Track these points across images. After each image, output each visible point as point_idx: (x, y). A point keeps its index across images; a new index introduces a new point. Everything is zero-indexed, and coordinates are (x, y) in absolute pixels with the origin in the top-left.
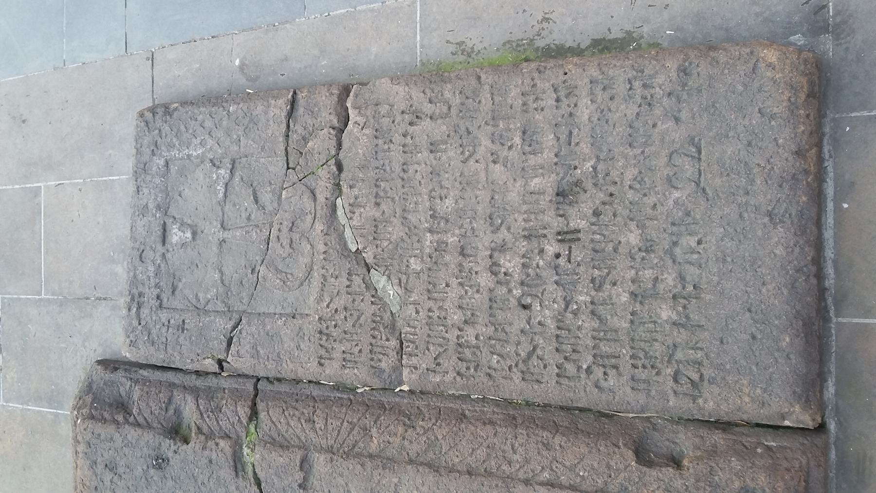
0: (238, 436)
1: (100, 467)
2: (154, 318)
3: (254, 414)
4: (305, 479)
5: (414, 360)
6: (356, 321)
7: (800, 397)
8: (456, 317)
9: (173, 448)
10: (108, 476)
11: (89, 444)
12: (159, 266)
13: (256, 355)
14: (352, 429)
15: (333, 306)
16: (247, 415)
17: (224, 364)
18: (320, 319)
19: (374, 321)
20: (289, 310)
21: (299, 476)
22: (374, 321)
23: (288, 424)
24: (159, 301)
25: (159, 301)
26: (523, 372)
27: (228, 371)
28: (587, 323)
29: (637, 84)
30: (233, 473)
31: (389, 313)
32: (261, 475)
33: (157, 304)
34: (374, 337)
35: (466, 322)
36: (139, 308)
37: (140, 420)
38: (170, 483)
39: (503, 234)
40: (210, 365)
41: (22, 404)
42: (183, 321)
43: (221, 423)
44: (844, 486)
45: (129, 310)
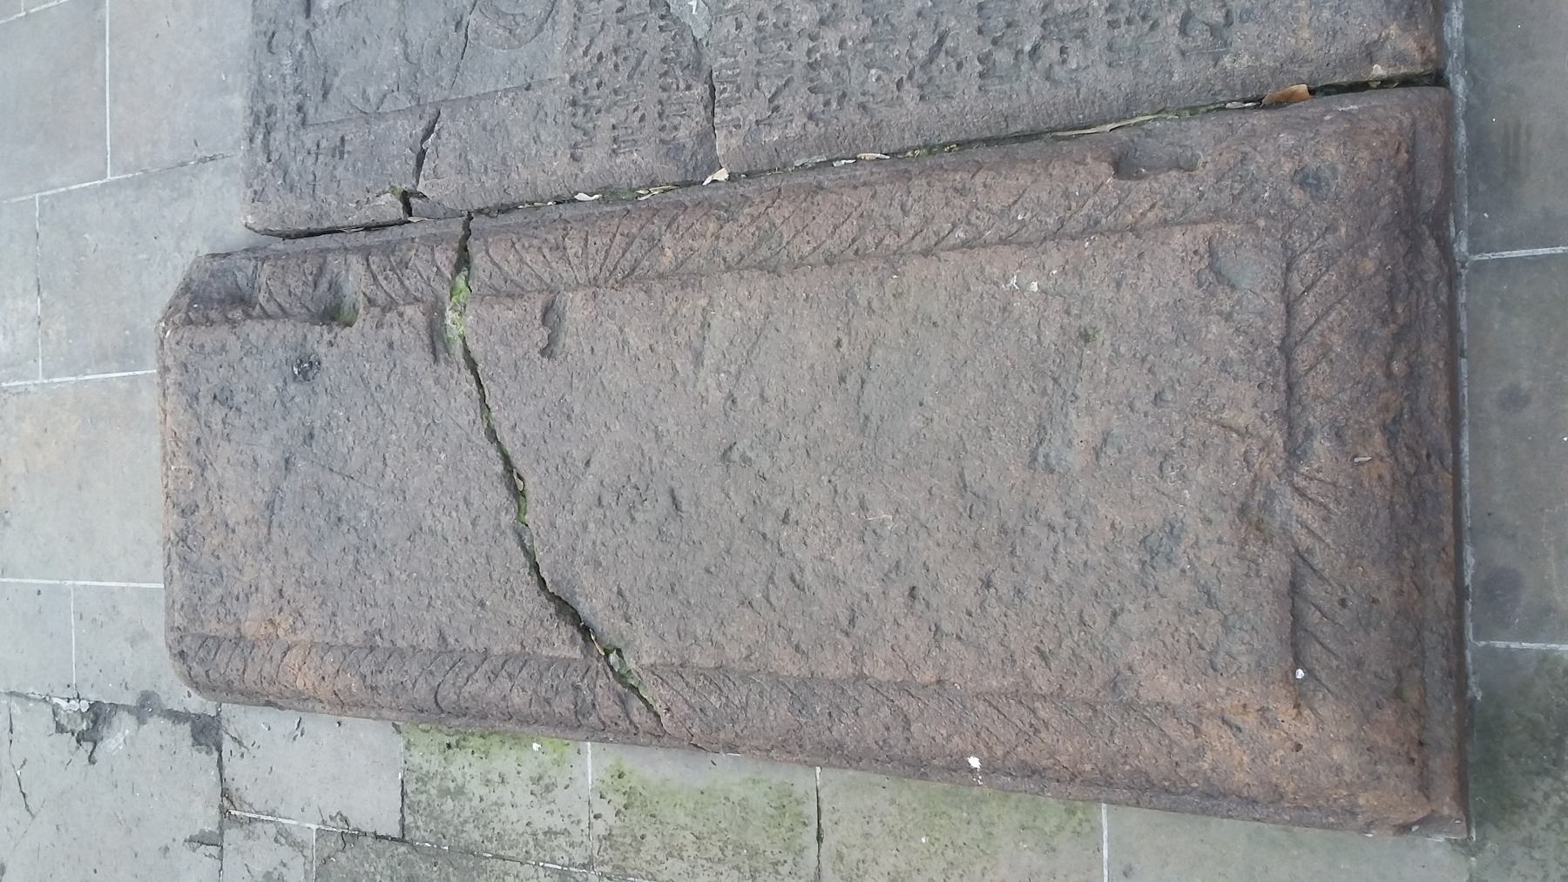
0: (437, 298)
1: (205, 401)
2: (293, 145)
3: (463, 261)
4: (552, 341)
5: (735, 112)
6: (634, 69)
7: (1397, 9)
9: (327, 337)
10: (218, 413)
11: (186, 366)
12: (301, 55)
13: (465, 168)
14: (630, 244)
15: (594, 51)
16: (451, 261)
17: (413, 201)
18: (573, 79)
19: (664, 61)
20: (520, 80)
21: (540, 336)
22: (664, 61)
23: (521, 260)
24: (301, 115)
25: (301, 115)
26: (921, 87)
27: (419, 215)
30: (430, 358)
31: (691, 42)
32: (476, 349)
33: (298, 119)
34: (664, 90)
35: (822, 22)
36: (268, 133)
37: (271, 308)
38: (324, 400)
40: (389, 206)
41: (75, 375)
42: (343, 139)
43: (407, 283)
44: (1482, 187)
45: (251, 141)
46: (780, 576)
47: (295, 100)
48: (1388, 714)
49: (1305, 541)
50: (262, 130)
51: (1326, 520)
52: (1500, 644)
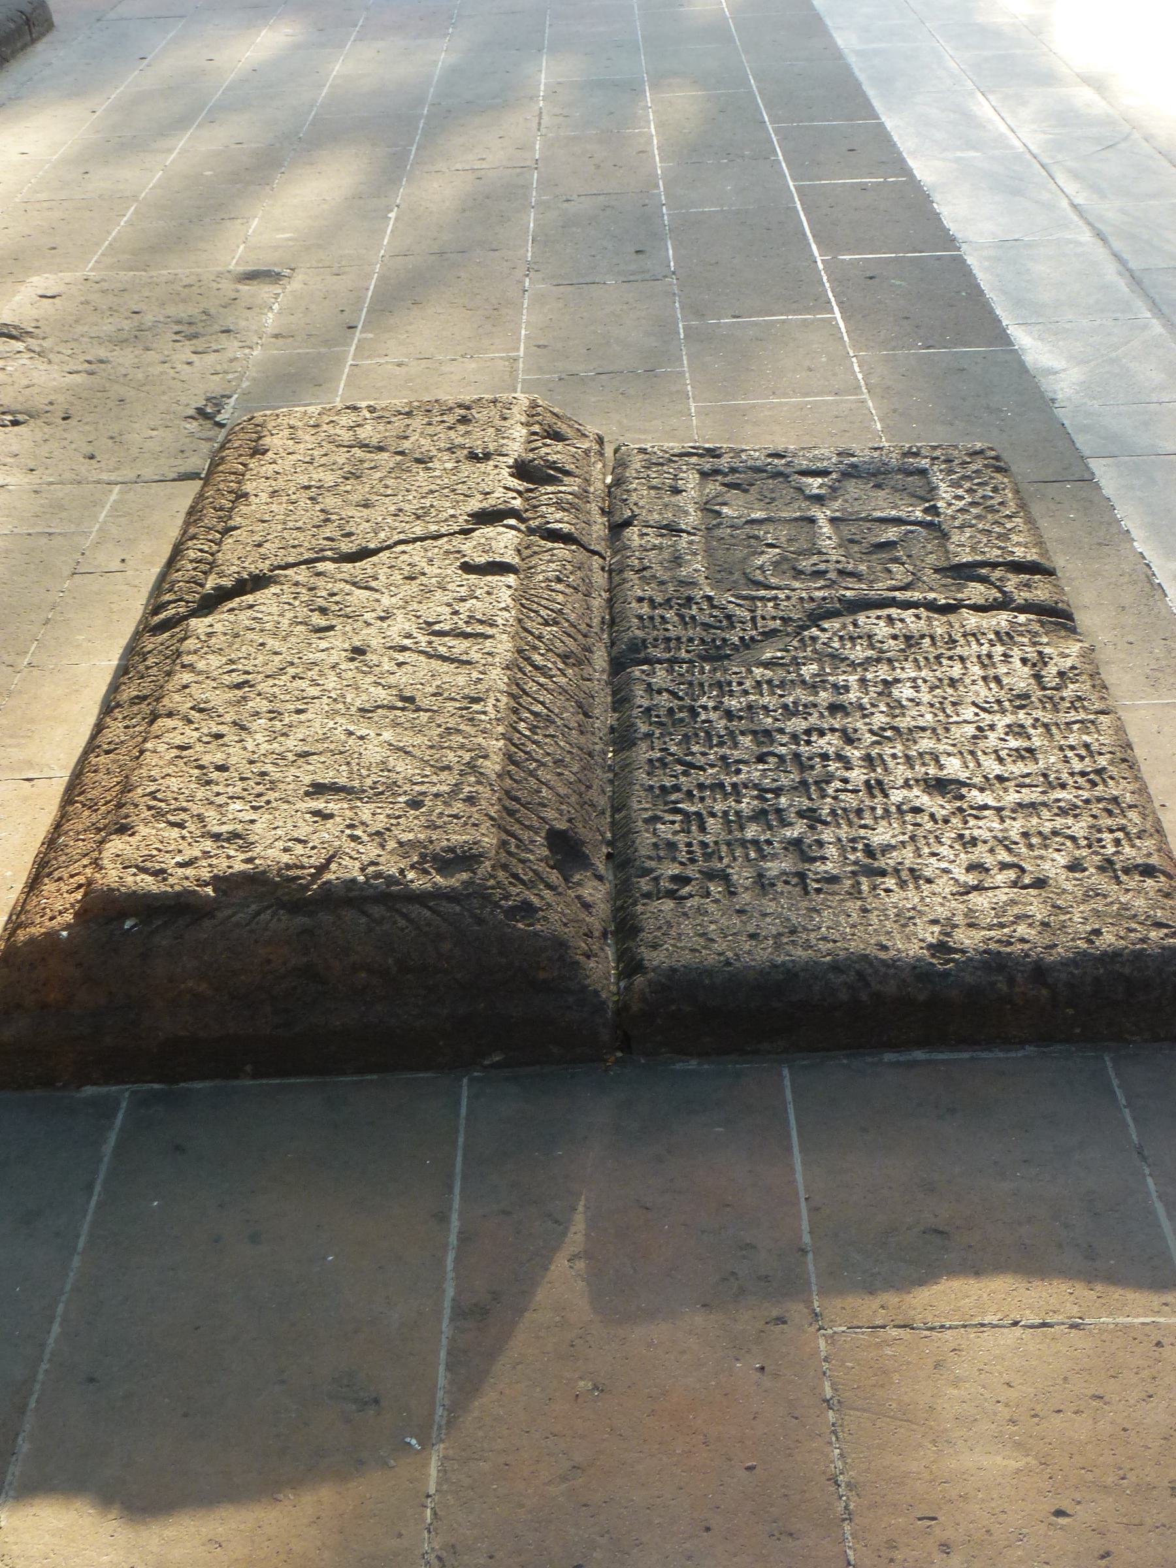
1: (463, 412)
8: (733, 703)
10: (450, 419)
19: (714, 640)
22: (714, 640)
28: (747, 804)
29: (1120, 835)
39: (869, 738)
46: (249, 677)
49: (220, 915)
51: (238, 925)
52: (124, 1105)
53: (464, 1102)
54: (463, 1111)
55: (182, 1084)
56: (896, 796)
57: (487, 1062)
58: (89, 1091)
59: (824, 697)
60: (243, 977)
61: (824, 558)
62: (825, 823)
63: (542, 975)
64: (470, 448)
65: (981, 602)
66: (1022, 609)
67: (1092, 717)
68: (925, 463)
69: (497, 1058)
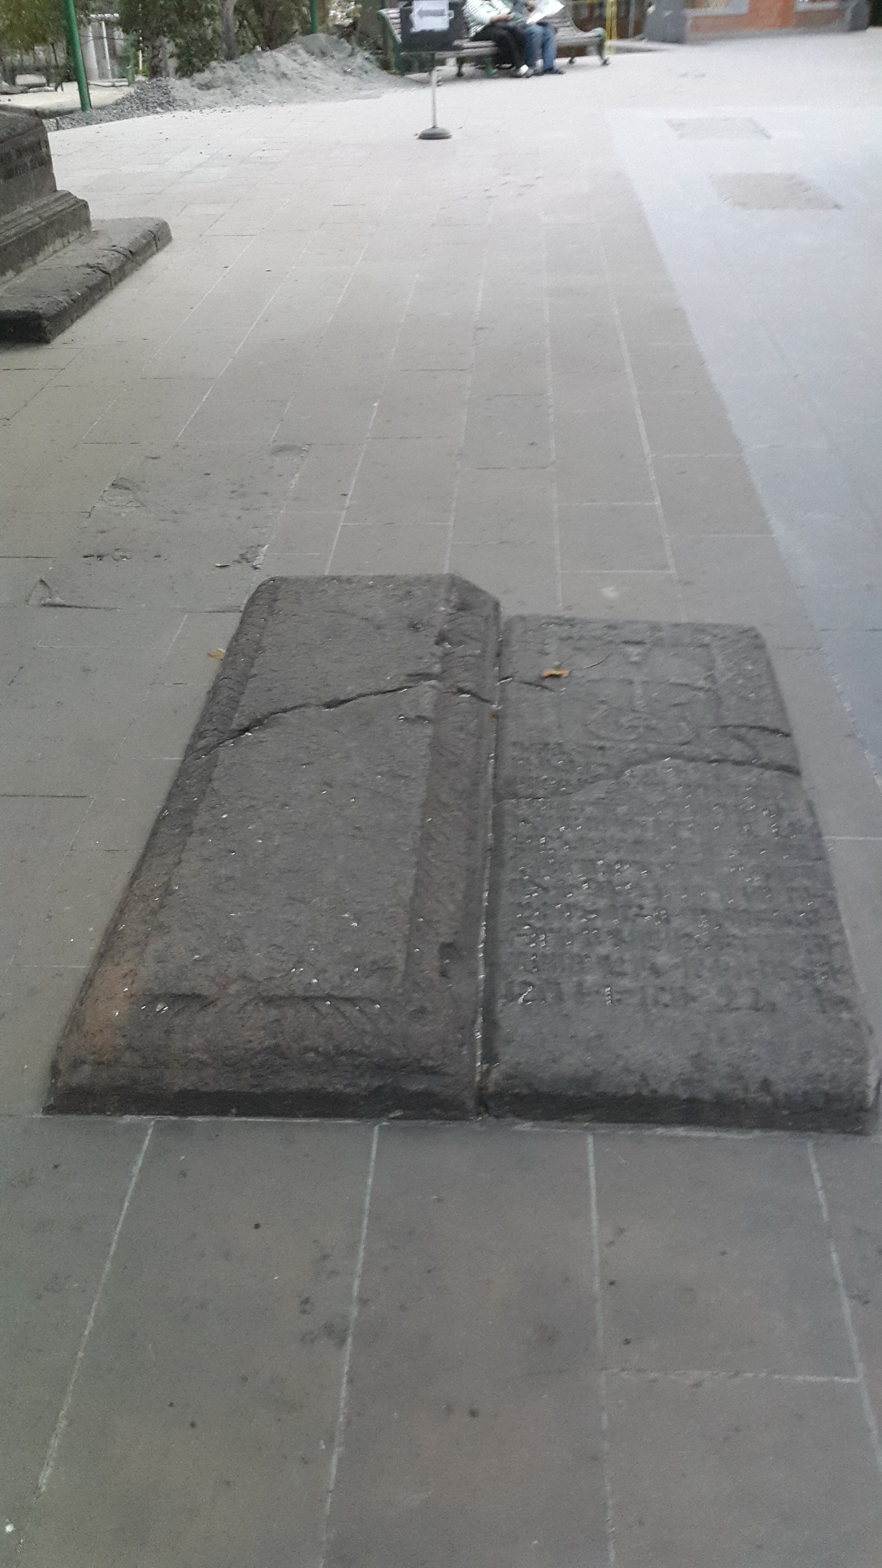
1: (407, 588)
39: (658, 871)
47: (576, 636)
48: (120, 1042)
49: (220, 1004)
50: (562, 622)
52: (150, 1131)
53: (375, 1147)
54: (373, 1155)
55: (190, 1118)
56: (676, 923)
57: (392, 1116)
58: (128, 1119)
59: (632, 834)
60: (233, 1052)
61: (638, 715)
62: (624, 942)
63: (430, 1063)
64: (412, 619)
65: (740, 759)
66: (766, 766)
67: (810, 864)
68: (707, 639)
69: (398, 1113)
